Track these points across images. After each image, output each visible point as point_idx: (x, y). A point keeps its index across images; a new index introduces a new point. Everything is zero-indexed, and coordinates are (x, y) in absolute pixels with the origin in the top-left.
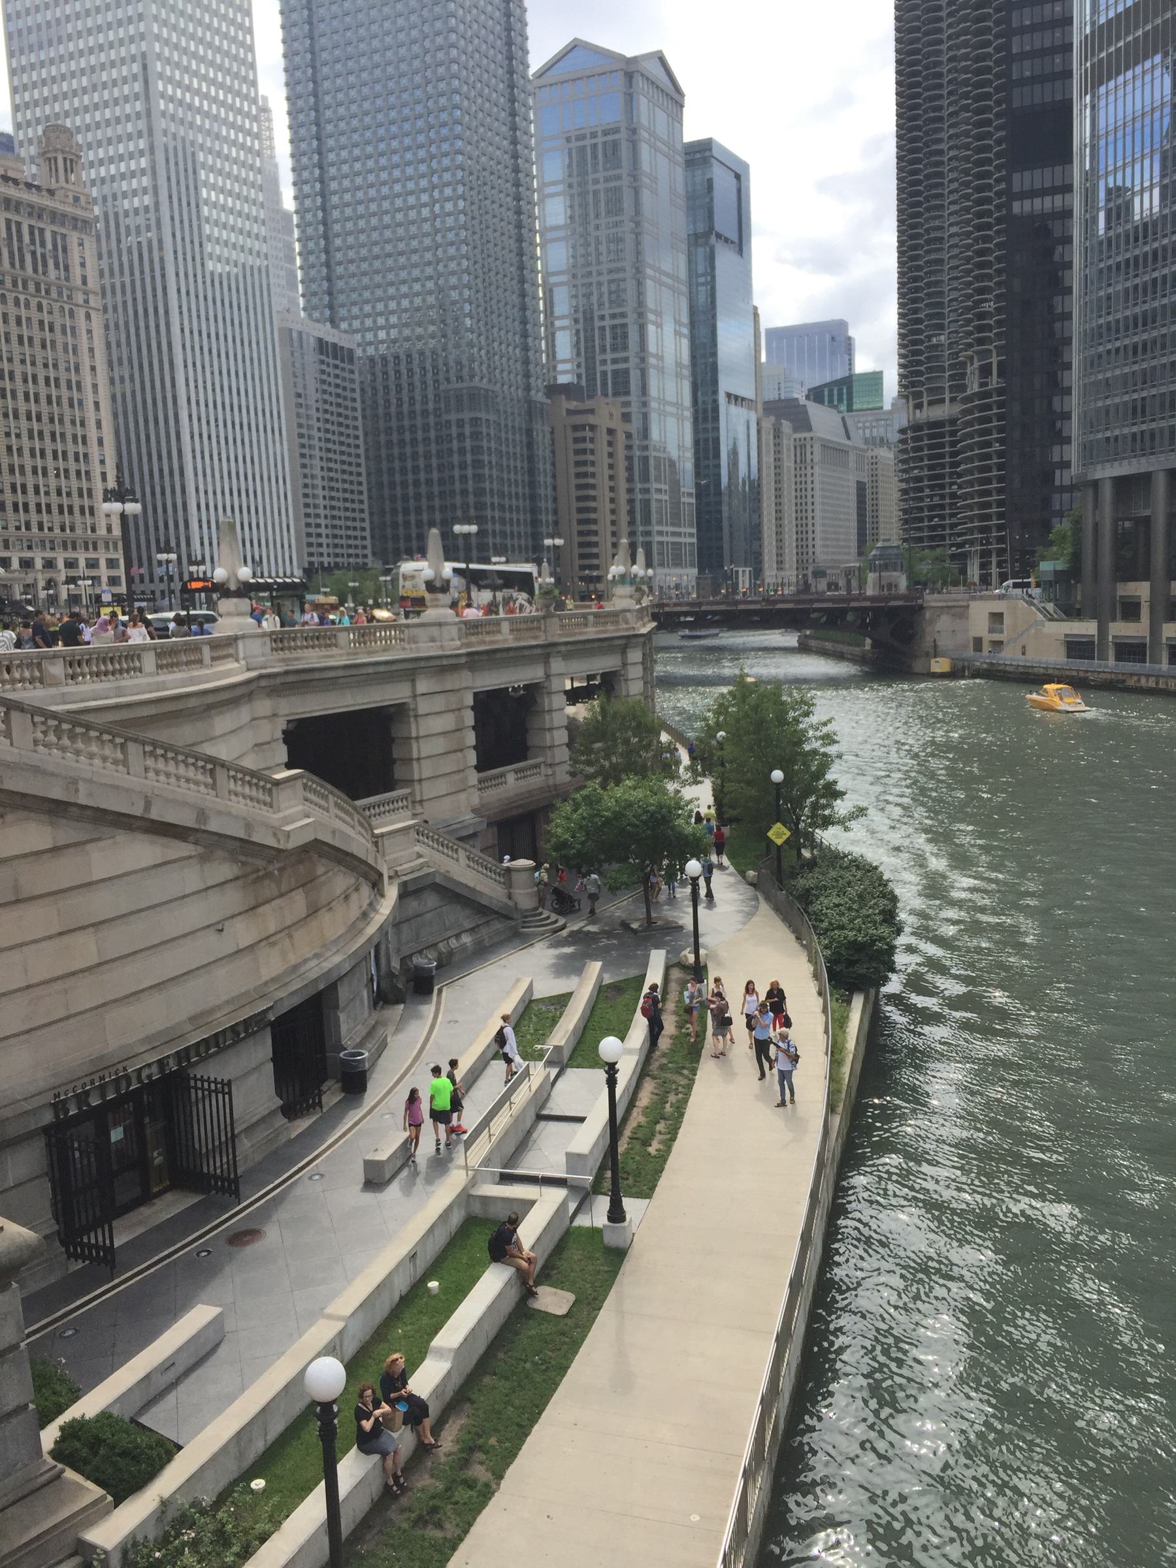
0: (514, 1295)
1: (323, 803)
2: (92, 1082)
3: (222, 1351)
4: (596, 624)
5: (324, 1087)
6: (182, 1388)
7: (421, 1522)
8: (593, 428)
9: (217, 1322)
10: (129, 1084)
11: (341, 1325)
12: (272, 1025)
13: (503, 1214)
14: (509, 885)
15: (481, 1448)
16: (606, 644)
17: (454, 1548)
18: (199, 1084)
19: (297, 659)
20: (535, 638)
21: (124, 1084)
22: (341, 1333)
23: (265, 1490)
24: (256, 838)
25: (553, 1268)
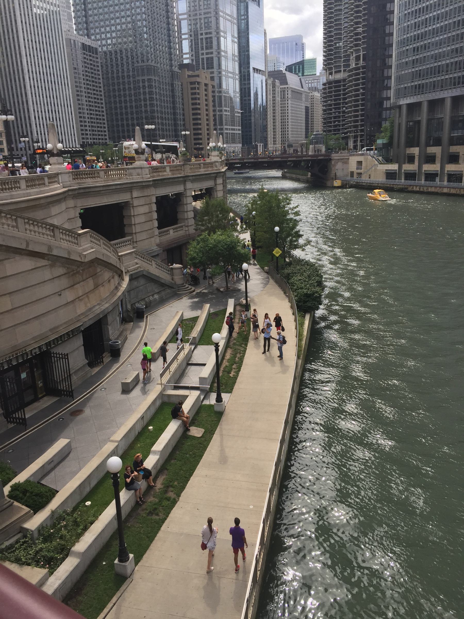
0: (181, 430)
1: (98, 243)
2: (13, 356)
3: (71, 455)
4: (204, 168)
5: (104, 355)
6: (57, 470)
7: (150, 513)
8: (199, 83)
9: (68, 445)
10: (27, 356)
11: (116, 444)
12: (82, 331)
13: (176, 401)
14: (172, 275)
15: (172, 486)
16: (208, 176)
17: (163, 522)
18: (55, 355)
19: (83, 183)
20: (180, 174)
21: (25, 356)
22: (117, 447)
23: (91, 505)
24: (72, 257)
25: (196, 420)
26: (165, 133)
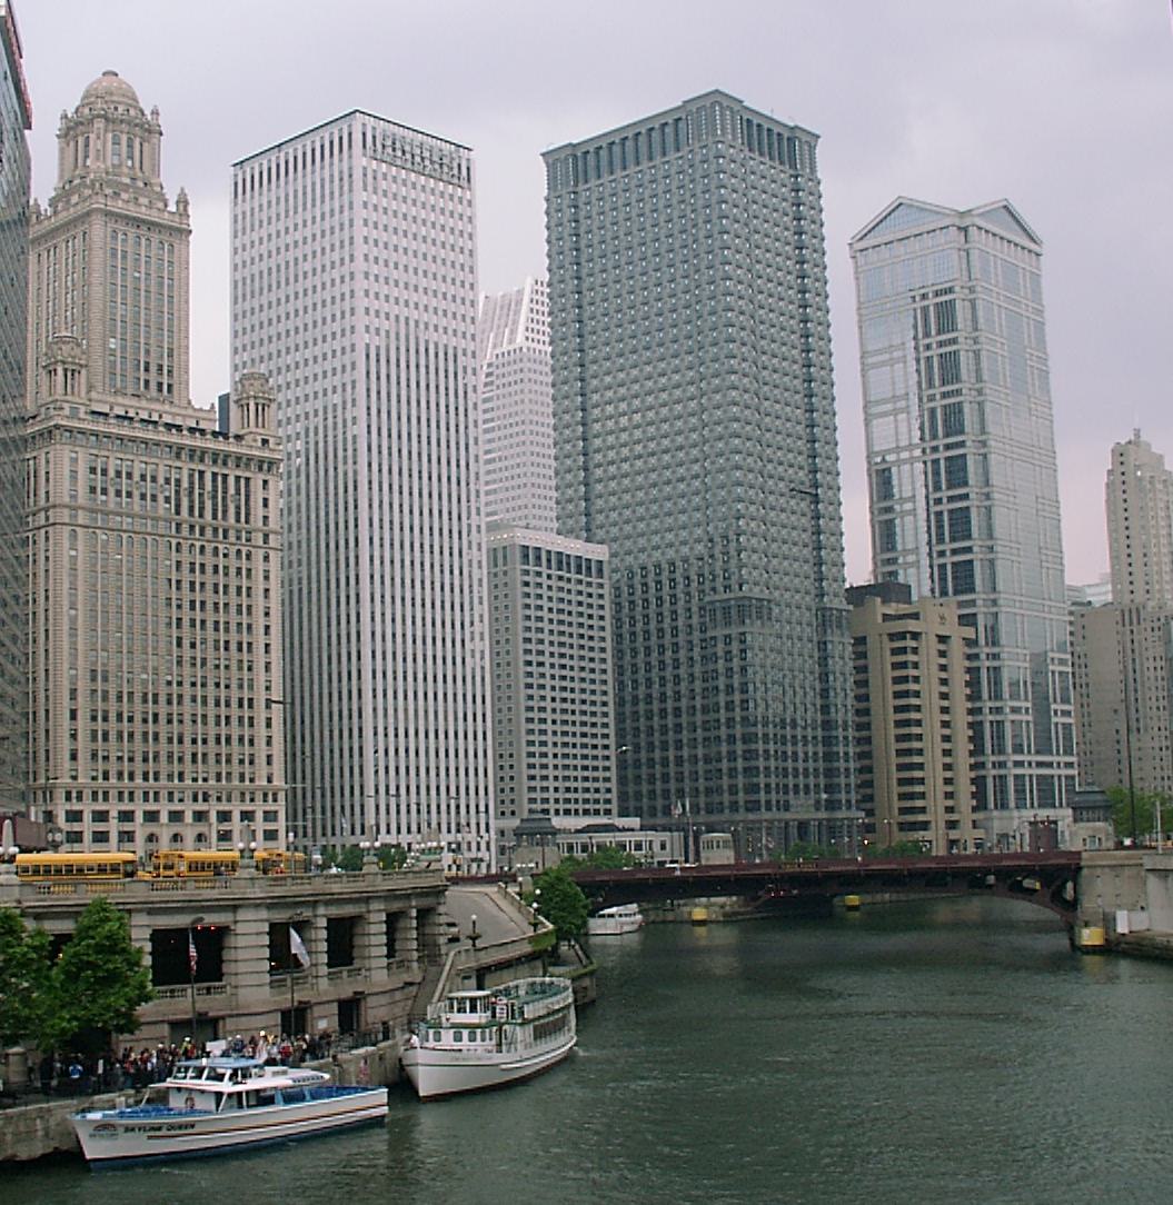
8: (916, 636)
26: (791, 781)
